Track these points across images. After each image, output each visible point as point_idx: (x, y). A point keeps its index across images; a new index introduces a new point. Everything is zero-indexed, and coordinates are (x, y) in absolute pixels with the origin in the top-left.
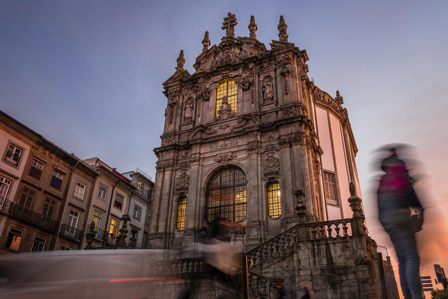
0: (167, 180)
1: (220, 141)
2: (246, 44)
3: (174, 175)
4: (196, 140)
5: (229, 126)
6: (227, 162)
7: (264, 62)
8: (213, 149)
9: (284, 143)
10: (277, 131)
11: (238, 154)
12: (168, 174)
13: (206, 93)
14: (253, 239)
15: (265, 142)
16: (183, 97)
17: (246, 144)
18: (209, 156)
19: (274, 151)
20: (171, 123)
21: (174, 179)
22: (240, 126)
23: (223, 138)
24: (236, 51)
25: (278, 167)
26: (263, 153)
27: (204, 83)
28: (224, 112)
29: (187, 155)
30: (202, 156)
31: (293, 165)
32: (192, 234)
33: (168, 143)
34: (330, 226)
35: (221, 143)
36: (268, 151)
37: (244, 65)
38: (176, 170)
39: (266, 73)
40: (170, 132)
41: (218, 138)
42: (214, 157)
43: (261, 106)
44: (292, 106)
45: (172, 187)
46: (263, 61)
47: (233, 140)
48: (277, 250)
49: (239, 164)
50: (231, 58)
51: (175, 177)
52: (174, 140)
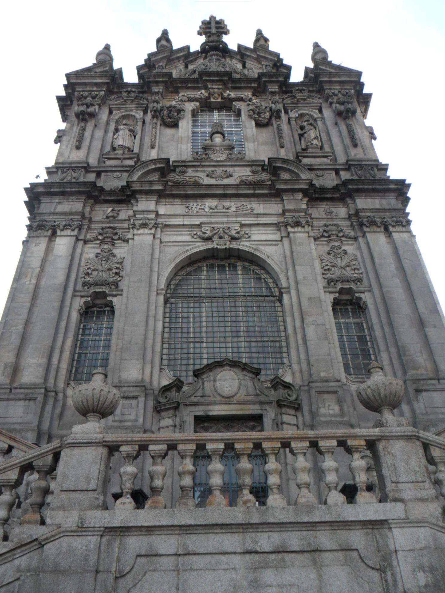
0: (60, 256)
1: (210, 200)
2: (253, 62)
3: (79, 251)
4: (151, 183)
6: (228, 243)
8: (191, 211)
9: (373, 223)
15: (318, 219)
17: (277, 215)
18: (181, 223)
19: (343, 239)
20: (78, 148)
22: (258, 179)
23: (220, 192)
25: (358, 270)
26: (318, 238)
28: (218, 148)
30: (160, 220)
32: (134, 397)
36: (329, 236)
37: (256, 85)
38: (86, 242)
41: (206, 190)
42: (191, 228)
47: (242, 203)
49: (260, 251)
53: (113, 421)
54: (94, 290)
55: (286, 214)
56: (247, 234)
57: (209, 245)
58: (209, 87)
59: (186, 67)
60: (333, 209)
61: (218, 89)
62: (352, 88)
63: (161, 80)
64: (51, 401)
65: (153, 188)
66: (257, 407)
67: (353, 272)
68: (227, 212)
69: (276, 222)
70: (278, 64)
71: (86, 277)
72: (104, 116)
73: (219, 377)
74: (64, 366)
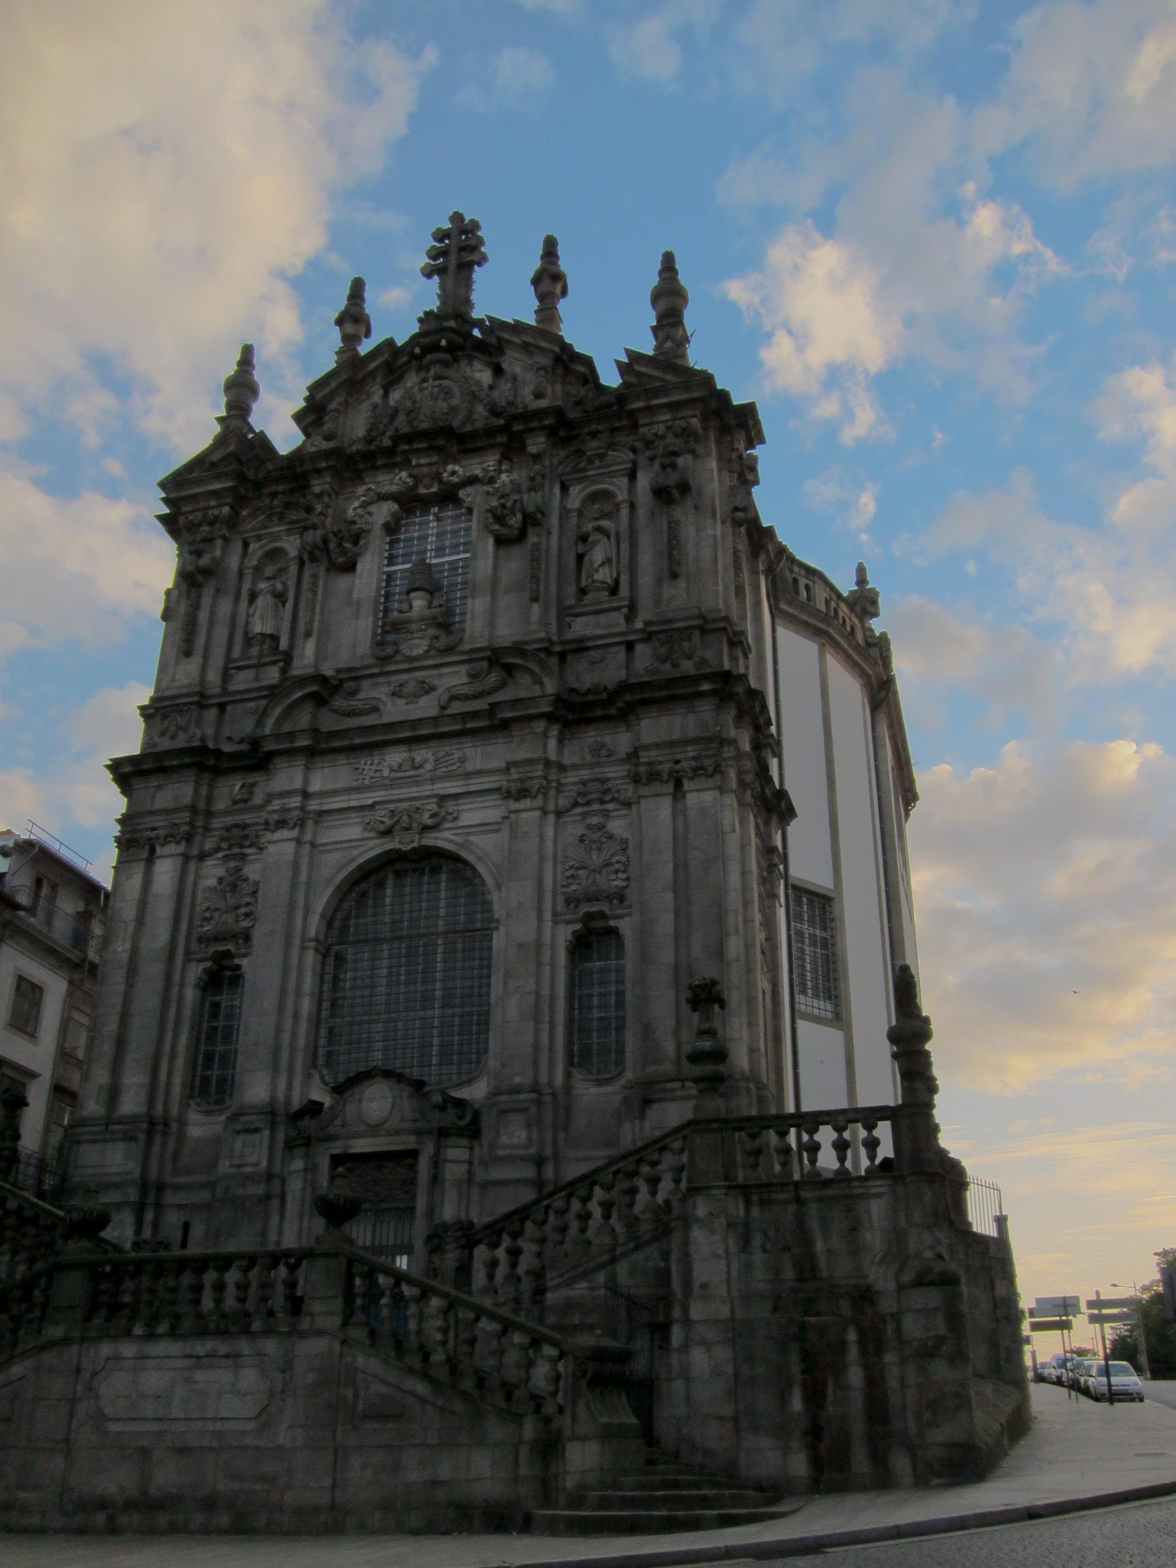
3: (191, 878)
4: (291, 735)
5: (433, 689)
6: (417, 836)
7: (588, 434)
8: (361, 777)
9: (654, 776)
10: (629, 726)
11: (461, 807)
12: (165, 871)
13: (342, 539)
14: (511, 1160)
15: (576, 767)
16: (246, 545)
18: (345, 805)
19: (610, 806)
20: (188, 653)
21: (190, 895)
24: (478, 375)
25: (624, 872)
26: (567, 811)
27: (337, 494)
28: (414, 627)
29: (251, 793)
31: (680, 866)
33: (173, 737)
34: (816, 1130)
35: (395, 757)
36: (588, 804)
38: (202, 857)
39: (594, 482)
40: (184, 691)
43: (565, 614)
44: (693, 627)
45: (184, 926)
46: (586, 430)
47: (447, 749)
48: (607, 1216)
50: (455, 402)
51: (195, 884)
52: (198, 725)
53: (232, 1166)
54: (215, 949)
55: (513, 770)
56: (451, 814)
57: (389, 846)
58: (414, 463)
59: (386, 395)
60: (608, 739)
61: (431, 464)
62: (698, 412)
63: (324, 465)
64: (158, 1140)
65: (296, 745)
66: (413, 1138)
67: (614, 877)
68: (417, 776)
69: (495, 785)
70: (565, 358)
71: (205, 924)
72: (234, 562)
73: (367, 1094)
74: (178, 1080)
